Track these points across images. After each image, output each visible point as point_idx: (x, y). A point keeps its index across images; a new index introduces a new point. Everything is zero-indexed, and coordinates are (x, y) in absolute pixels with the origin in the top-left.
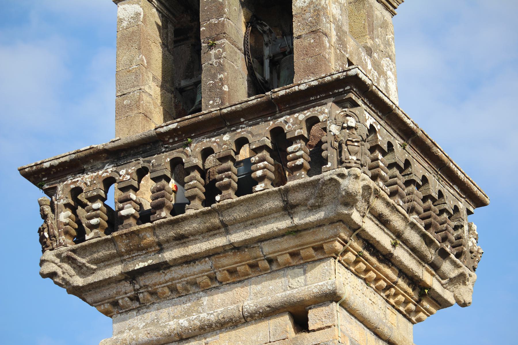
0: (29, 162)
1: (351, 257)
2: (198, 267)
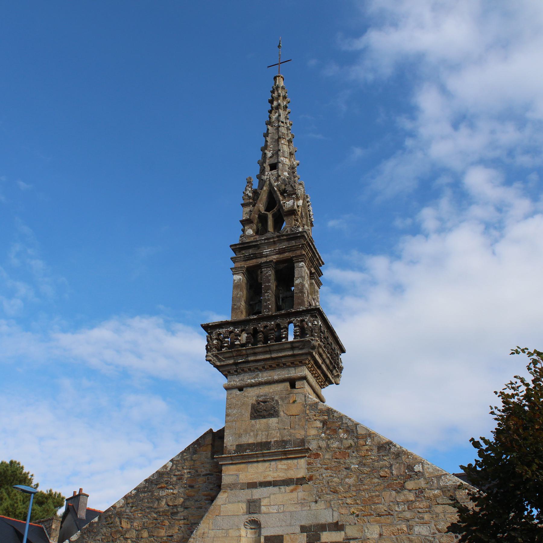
0: (205, 322)
1: (310, 366)
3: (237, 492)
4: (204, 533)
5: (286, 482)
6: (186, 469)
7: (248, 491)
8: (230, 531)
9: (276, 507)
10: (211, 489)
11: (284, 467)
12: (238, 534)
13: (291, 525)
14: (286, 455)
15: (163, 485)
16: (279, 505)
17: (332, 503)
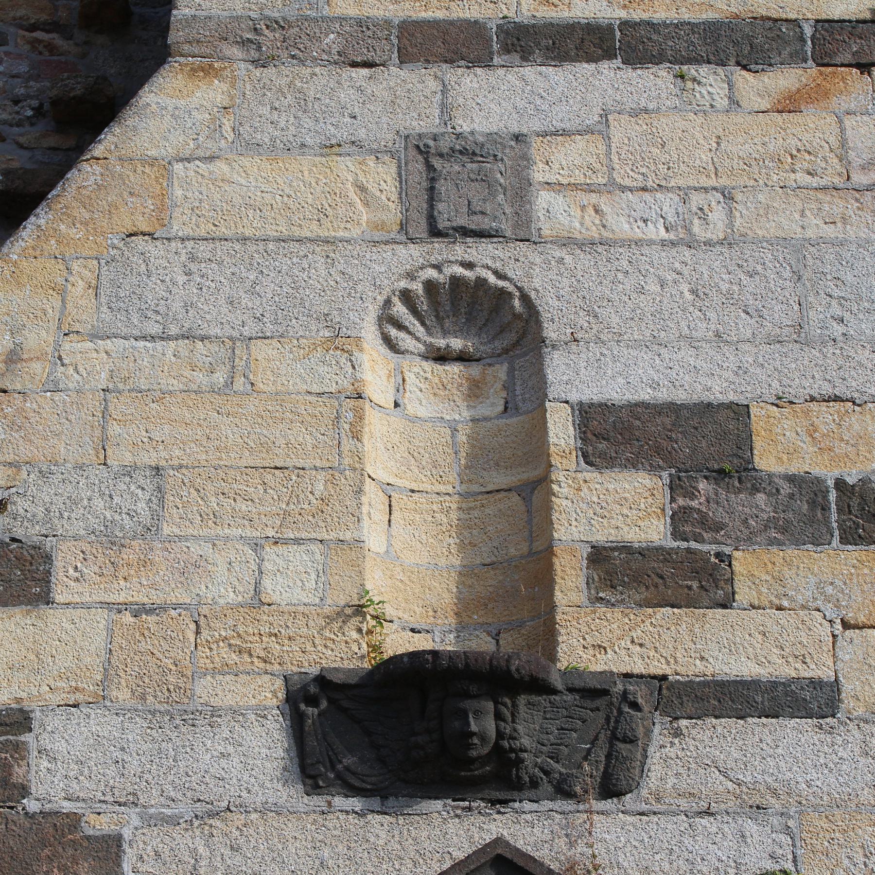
3: (319, 80)
8: (262, 351)
9: (668, 203)
12: (331, 376)
13: (799, 334)
16: (684, 194)
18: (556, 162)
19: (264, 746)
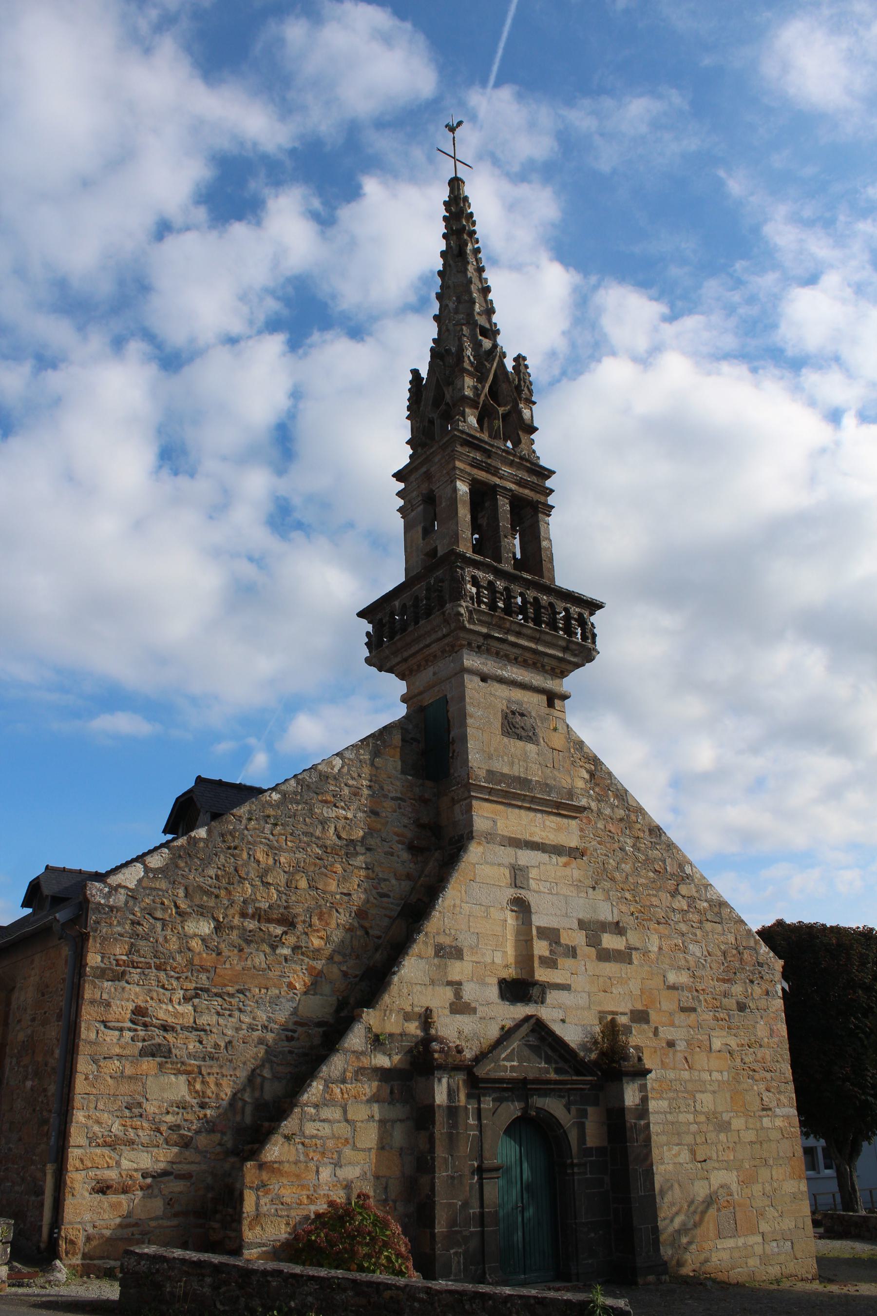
2: (515, 650)
4: (454, 906)
5: (557, 850)
6: (365, 780)
7: (510, 850)
8: (492, 909)
10: (405, 826)
11: (553, 825)
14: (558, 809)
15: (329, 798)
17: (611, 893)
18: (533, 873)
19: (493, 992)
